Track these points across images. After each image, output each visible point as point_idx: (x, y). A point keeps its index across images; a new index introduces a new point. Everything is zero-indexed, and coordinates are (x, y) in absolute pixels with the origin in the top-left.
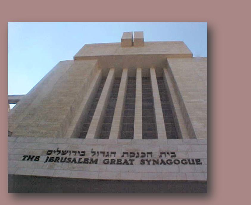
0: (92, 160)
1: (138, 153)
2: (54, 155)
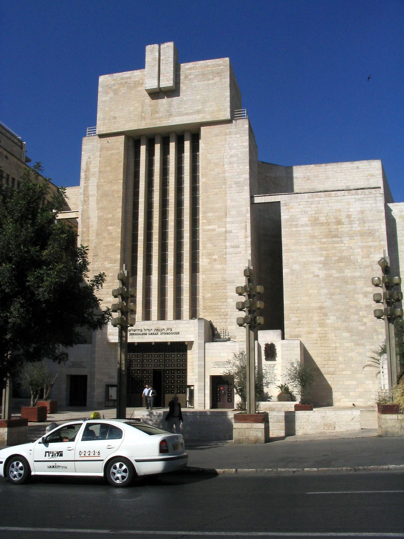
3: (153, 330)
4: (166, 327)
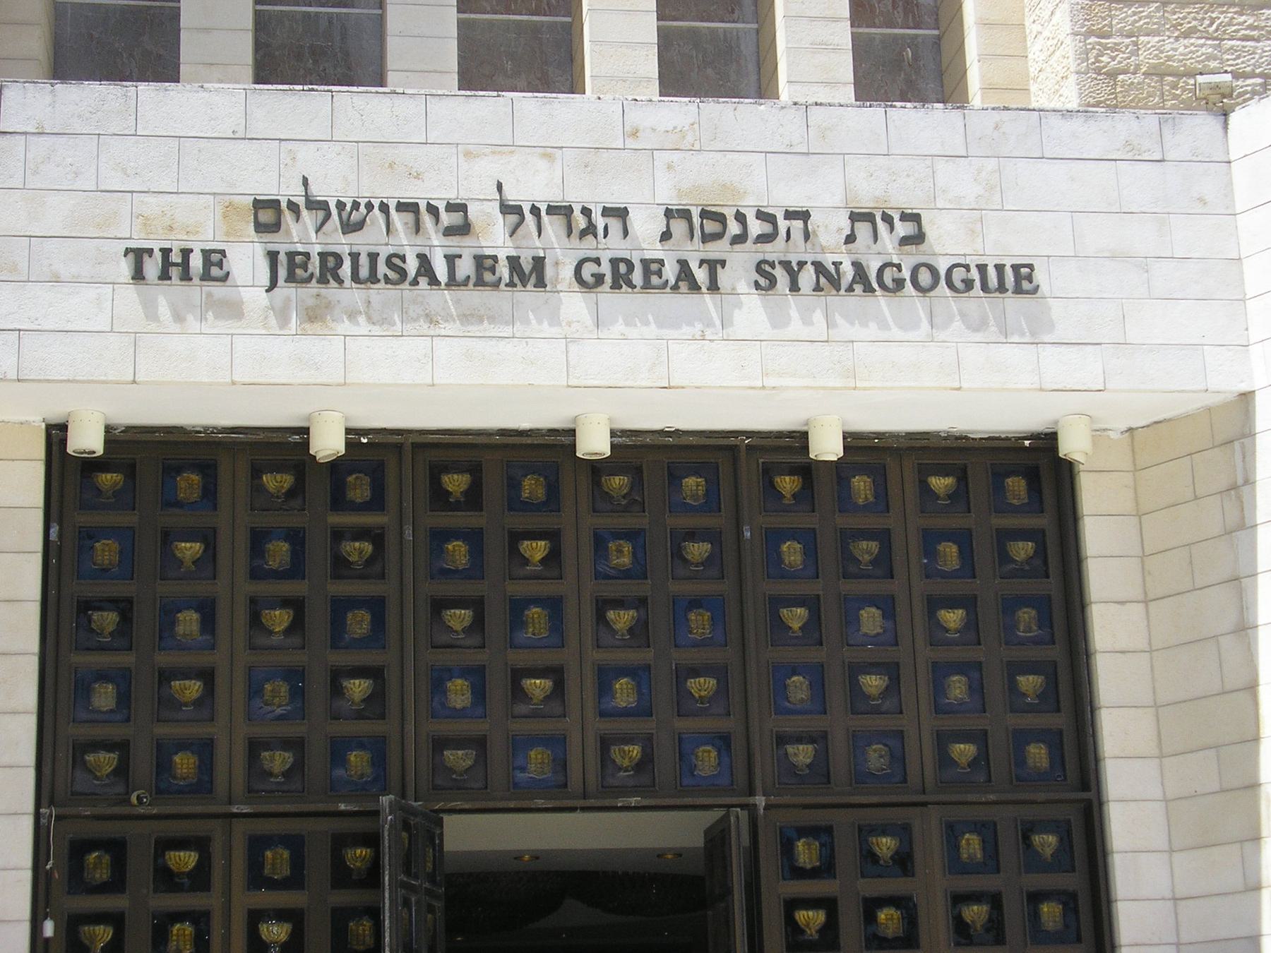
0: (514, 262)
1: (740, 218)
3: (645, 225)
4: (838, 200)
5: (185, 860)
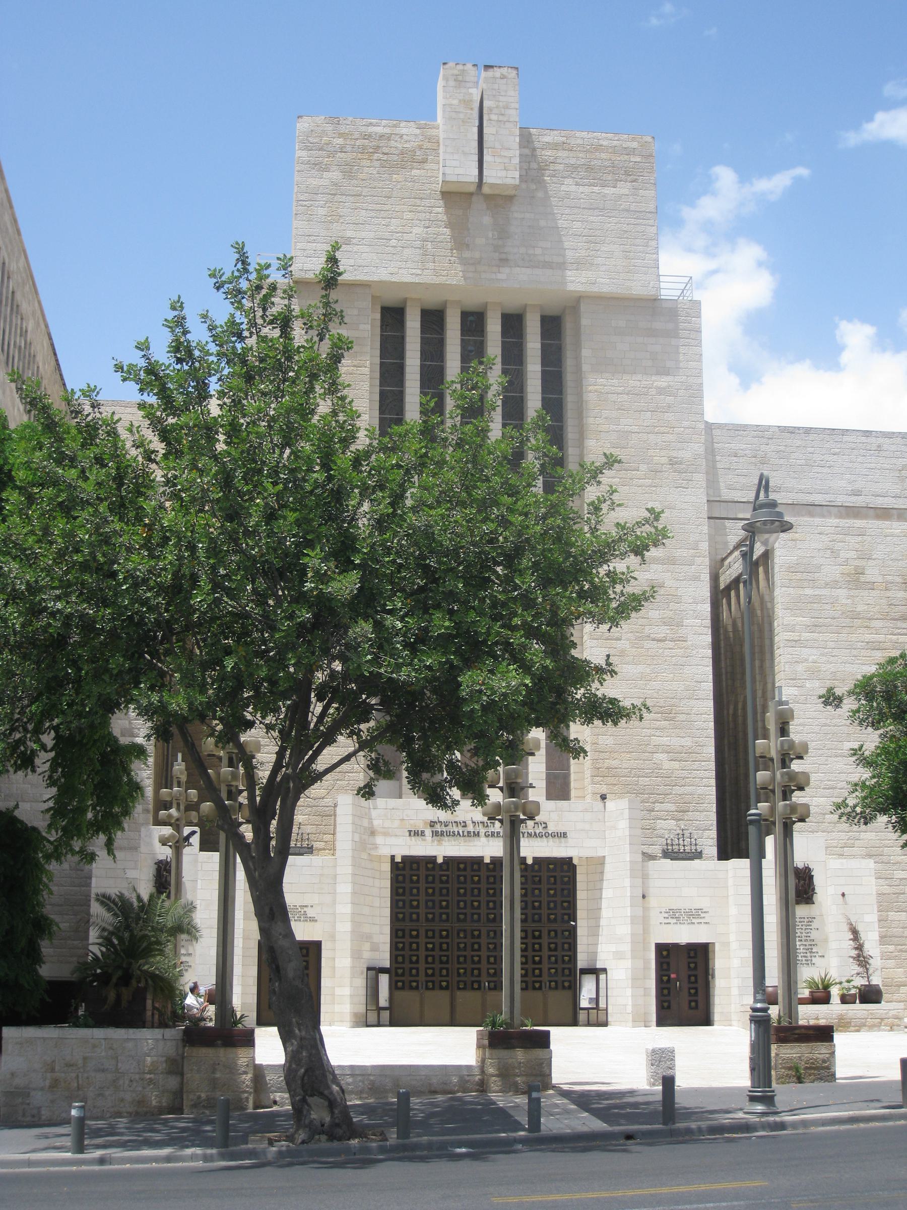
2: (438, 828)
5: (414, 933)
